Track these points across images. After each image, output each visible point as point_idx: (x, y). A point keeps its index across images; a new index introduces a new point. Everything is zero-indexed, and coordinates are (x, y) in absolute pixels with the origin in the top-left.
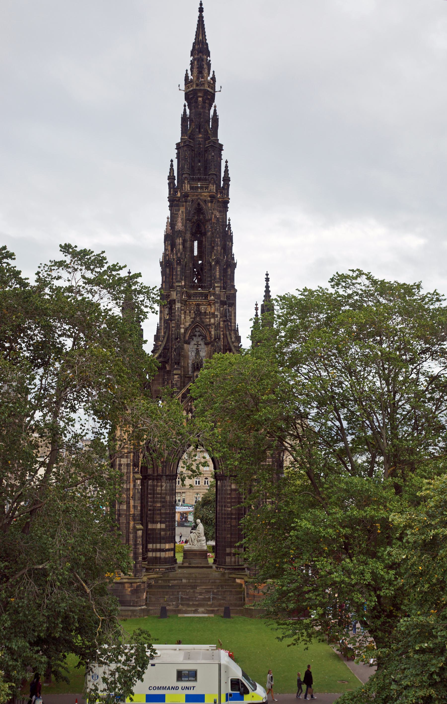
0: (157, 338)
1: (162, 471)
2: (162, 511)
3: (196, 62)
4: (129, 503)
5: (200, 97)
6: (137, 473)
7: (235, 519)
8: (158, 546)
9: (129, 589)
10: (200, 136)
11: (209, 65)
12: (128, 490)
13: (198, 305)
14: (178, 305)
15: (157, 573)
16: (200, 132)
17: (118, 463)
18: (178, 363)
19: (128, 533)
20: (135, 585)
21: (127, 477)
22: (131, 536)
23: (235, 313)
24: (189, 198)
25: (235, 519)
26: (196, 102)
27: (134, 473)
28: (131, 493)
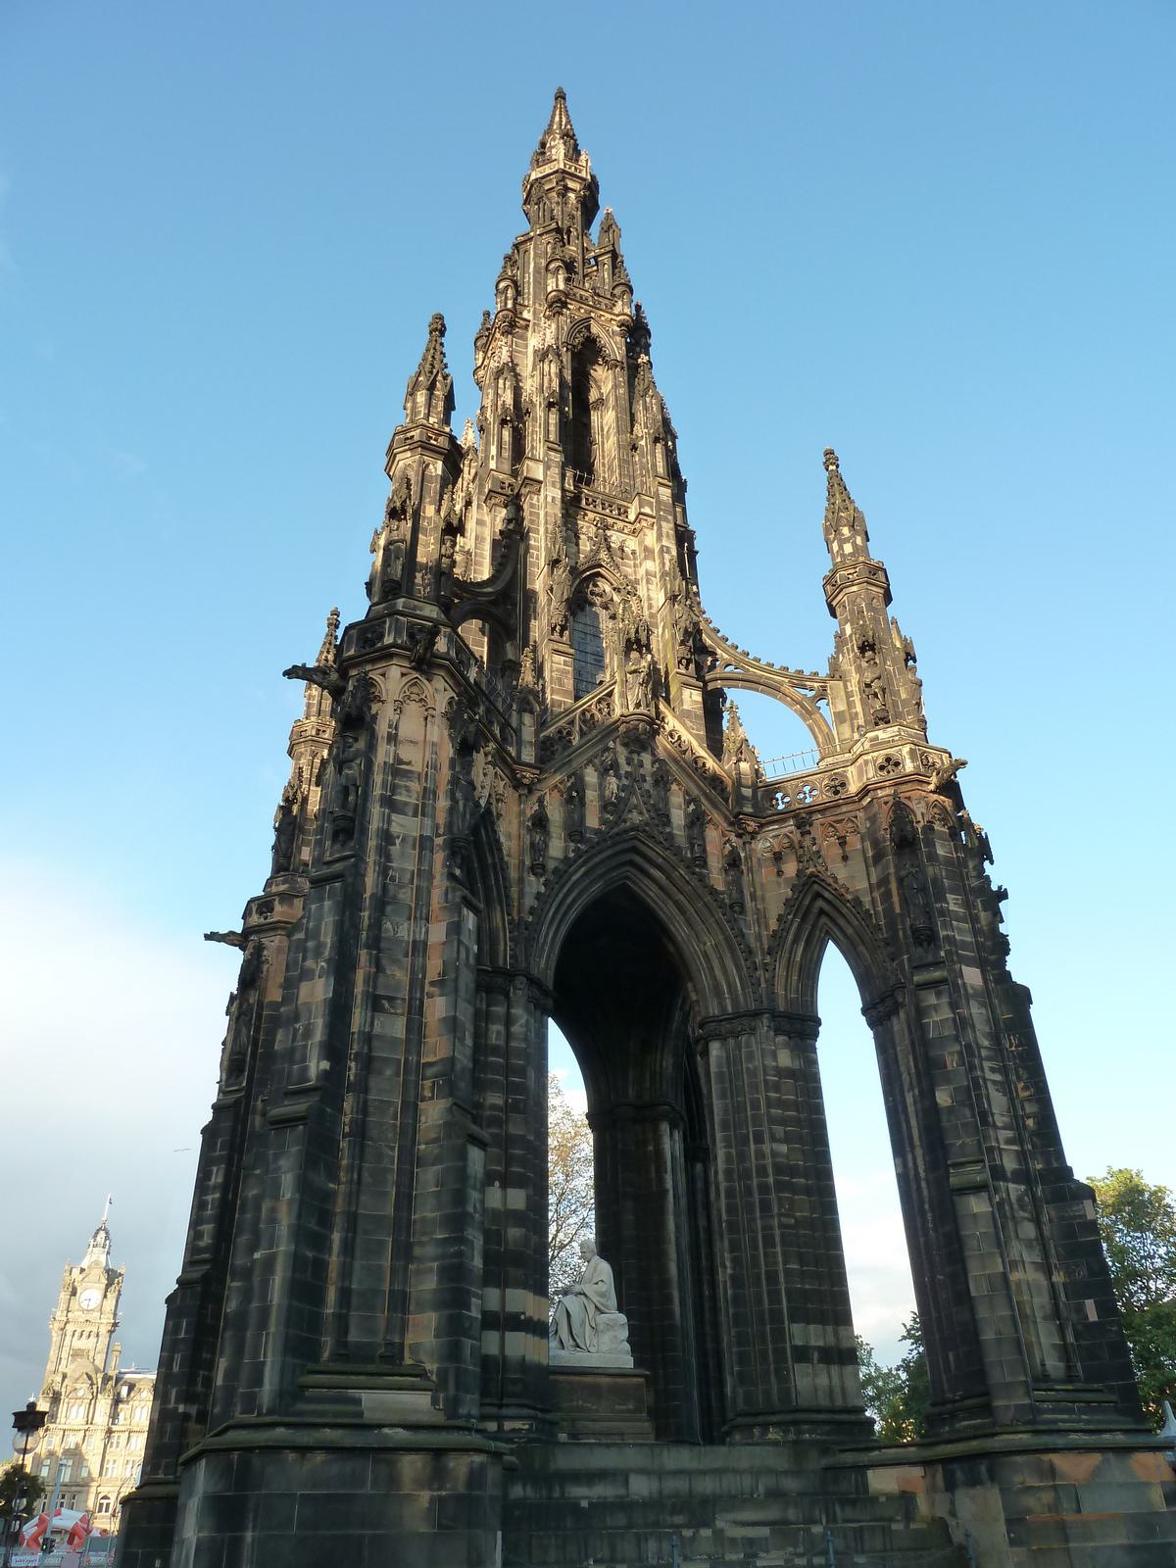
5: (573, 190)
9: (425, 1497)
12: (420, 948)
17: (375, 824)
19: (410, 1160)
22: (428, 1178)
28: (434, 966)
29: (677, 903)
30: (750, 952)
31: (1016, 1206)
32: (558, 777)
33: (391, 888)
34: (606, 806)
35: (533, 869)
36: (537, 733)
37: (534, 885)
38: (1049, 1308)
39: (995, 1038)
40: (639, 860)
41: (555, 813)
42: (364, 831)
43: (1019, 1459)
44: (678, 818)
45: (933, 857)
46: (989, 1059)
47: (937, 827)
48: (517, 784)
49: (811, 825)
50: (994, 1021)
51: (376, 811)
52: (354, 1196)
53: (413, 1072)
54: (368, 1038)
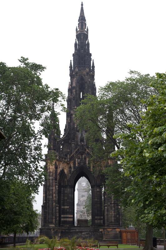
0: (65, 130)
3: (80, 24)
4: (53, 195)
6: (57, 183)
7: (99, 204)
8: (66, 216)
10: (82, 51)
11: (86, 25)
15: (65, 227)
16: (82, 49)
18: (74, 139)
19: (53, 208)
20: (55, 230)
21: (52, 184)
22: (54, 209)
24: (78, 74)
25: (99, 204)
26: (81, 38)
27: (55, 183)
28: (54, 191)
30: (95, 178)
34: (78, 163)
37: (70, 175)
41: (72, 165)
44: (87, 162)
48: (67, 164)
52: (48, 211)
53: (52, 201)
54: (49, 198)
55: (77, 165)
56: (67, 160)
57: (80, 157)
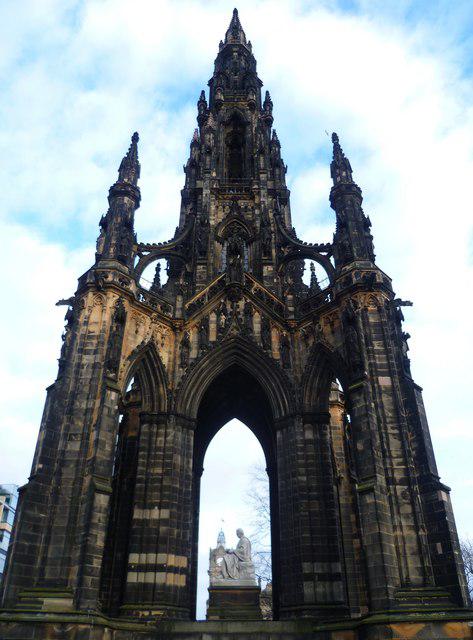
1: (169, 406)
2: (165, 483)
4: (88, 439)
8: (152, 558)
13: (235, 199)
14: (206, 192)
23: (289, 214)
25: (317, 498)
28: (95, 417)
29: (258, 368)
31: (400, 498)
32: (196, 321)
33: (81, 388)
34: (219, 329)
35: (181, 366)
36: (183, 304)
37: (180, 372)
38: (416, 548)
39: (396, 411)
40: (239, 352)
41: (193, 337)
42: (69, 365)
43: (378, 627)
44: (257, 327)
45: (366, 323)
46: (391, 422)
47: (371, 308)
48: (174, 329)
49: (319, 319)
50: (395, 403)
51: (75, 354)
55: (213, 338)
56: (174, 314)
57: (229, 307)
